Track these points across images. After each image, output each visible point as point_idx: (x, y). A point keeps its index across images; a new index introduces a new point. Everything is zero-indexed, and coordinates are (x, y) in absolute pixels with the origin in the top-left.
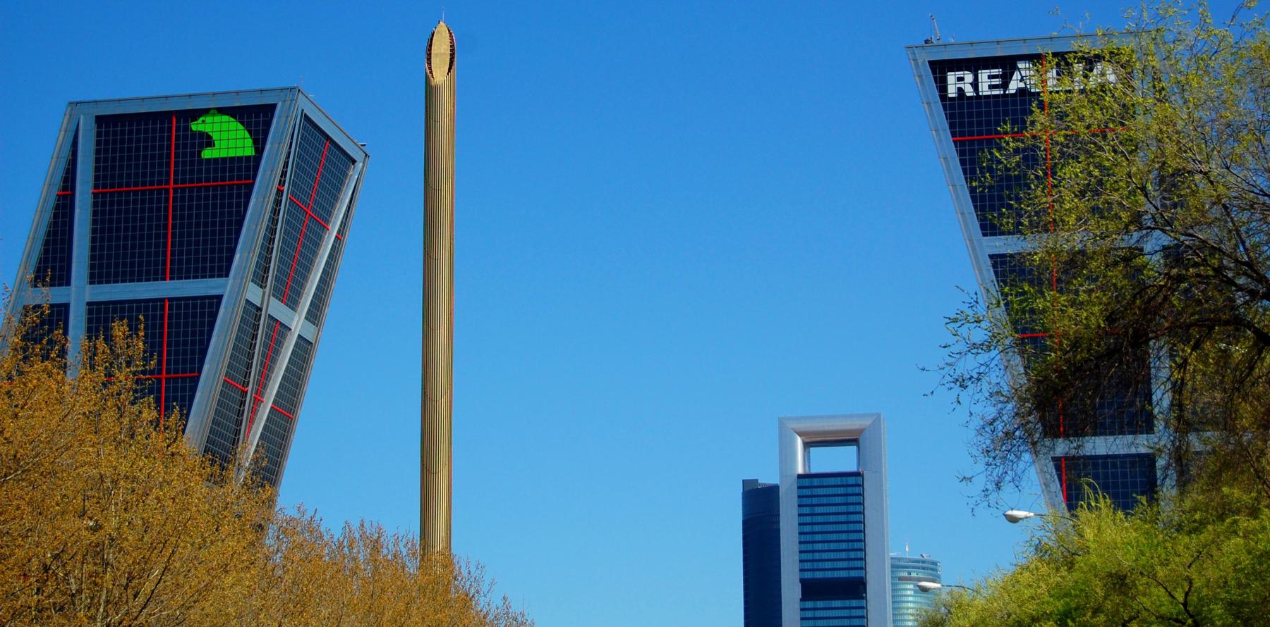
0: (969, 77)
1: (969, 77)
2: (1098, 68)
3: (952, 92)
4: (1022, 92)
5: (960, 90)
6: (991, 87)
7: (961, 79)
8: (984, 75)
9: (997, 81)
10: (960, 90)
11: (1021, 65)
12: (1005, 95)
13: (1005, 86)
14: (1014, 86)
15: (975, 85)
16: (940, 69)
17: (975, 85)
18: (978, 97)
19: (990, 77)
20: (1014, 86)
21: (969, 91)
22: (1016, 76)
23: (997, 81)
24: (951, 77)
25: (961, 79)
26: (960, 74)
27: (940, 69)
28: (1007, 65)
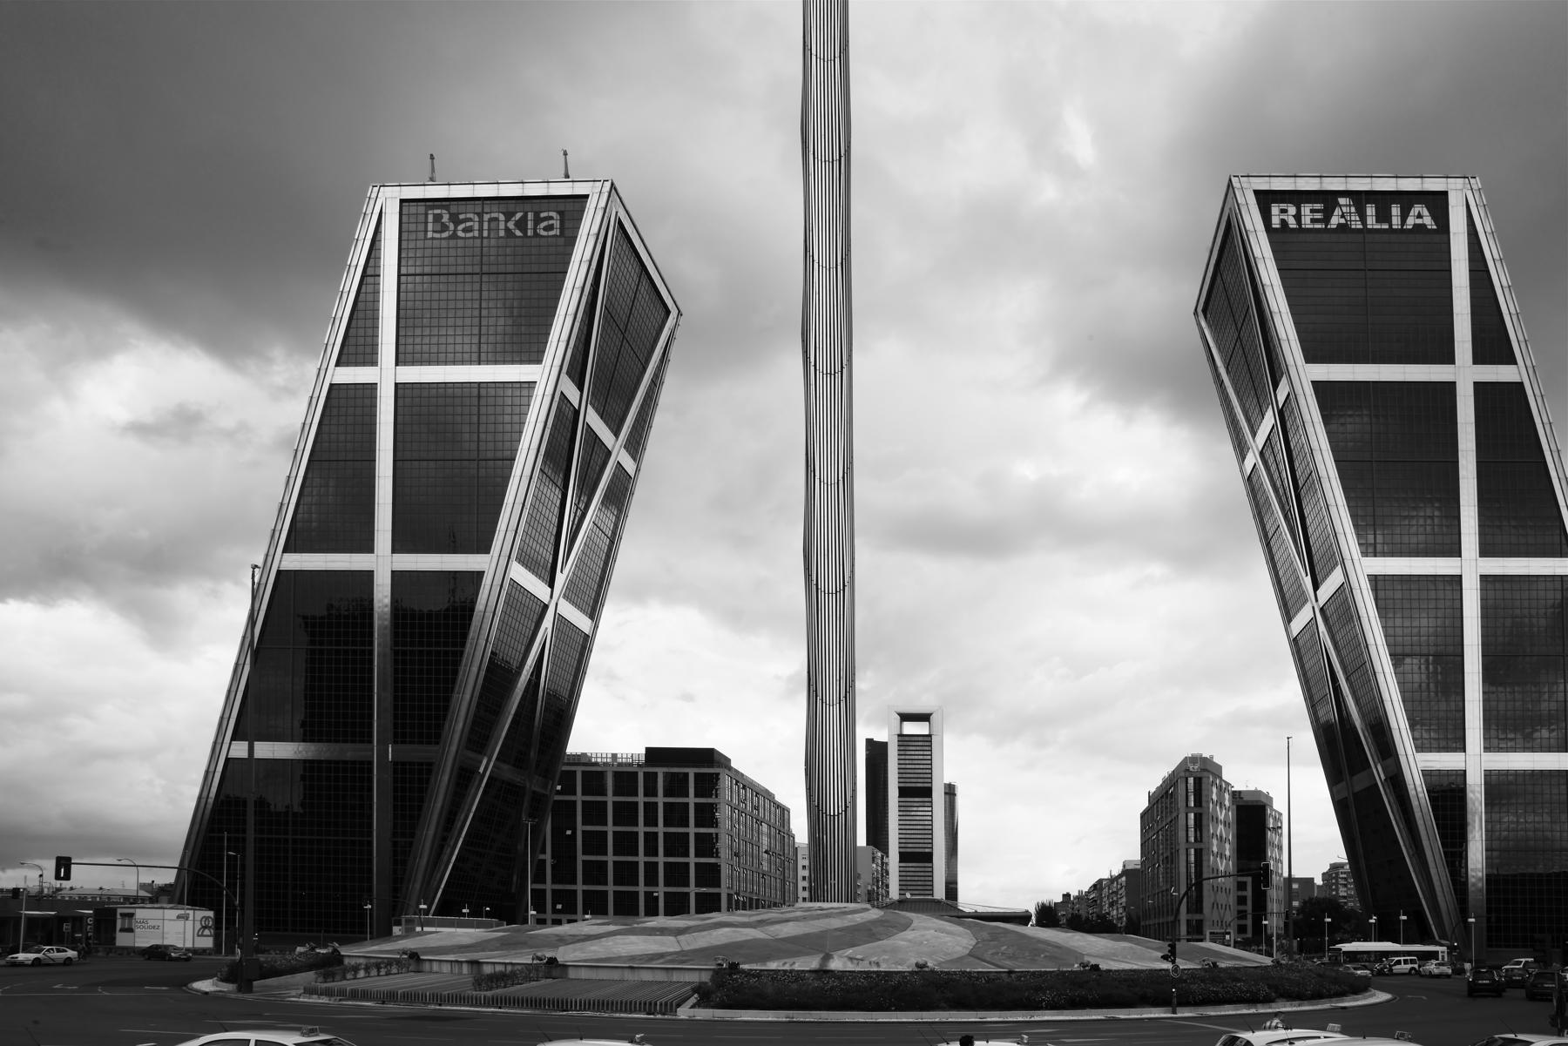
0: (1292, 210)
1: (1292, 210)
2: (1417, 209)
3: (1276, 222)
4: (1343, 228)
5: (1284, 222)
6: (1313, 221)
7: (1284, 211)
8: (1306, 209)
9: (1318, 216)
10: (1284, 222)
11: (1342, 201)
12: (1326, 230)
13: (1327, 220)
14: (1335, 221)
15: (1298, 217)
16: (1266, 199)
17: (1298, 217)
18: (1300, 230)
19: (1312, 211)
20: (1335, 221)
21: (1292, 223)
22: (1337, 212)
23: (1318, 216)
24: (1275, 209)
25: (1284, 211)
26: (1283, 206)
27: (1266, 199)
28: (1328, 199)
